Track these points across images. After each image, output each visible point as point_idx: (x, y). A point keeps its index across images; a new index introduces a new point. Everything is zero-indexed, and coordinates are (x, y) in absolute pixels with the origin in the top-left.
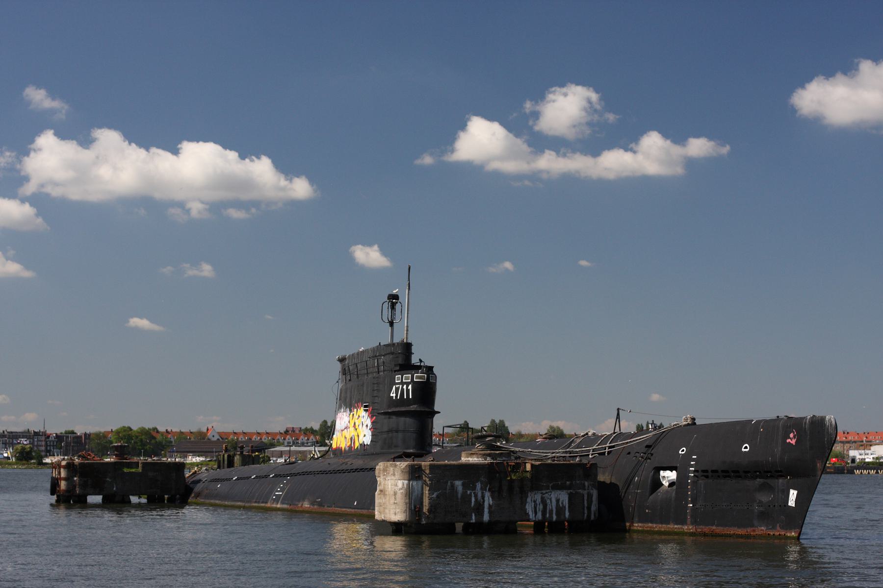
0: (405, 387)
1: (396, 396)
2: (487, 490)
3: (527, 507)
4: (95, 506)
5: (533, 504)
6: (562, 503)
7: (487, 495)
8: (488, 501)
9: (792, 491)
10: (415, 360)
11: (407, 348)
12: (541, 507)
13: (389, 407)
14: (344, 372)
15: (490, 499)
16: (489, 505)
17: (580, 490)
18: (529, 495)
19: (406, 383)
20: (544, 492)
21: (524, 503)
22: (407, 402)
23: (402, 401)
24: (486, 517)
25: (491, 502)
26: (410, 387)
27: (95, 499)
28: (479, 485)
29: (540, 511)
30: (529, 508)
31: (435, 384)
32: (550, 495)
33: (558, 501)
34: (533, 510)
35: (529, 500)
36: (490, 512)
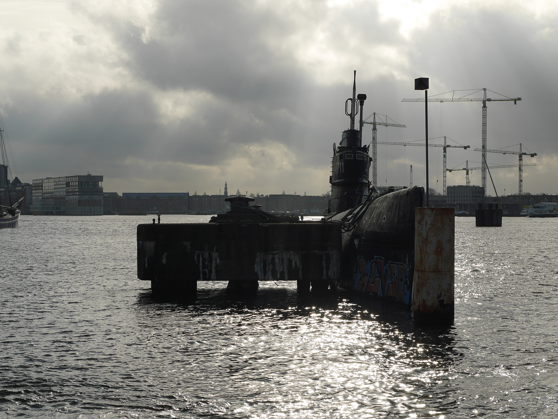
2: (215, 251)
3: (256, 266)
5: (262, 264)
6: (296, 263)
7: (215, 255)
12: (271, 267)
15: (218, 259)
16: (216, 264)
17: (315, 251)
18: (258, 255)
20: (275, 252)
25: (218, 261)
29: (270, 270)
32: (282, 256)
33: (290, 261)
34: (262, 270)
35: (258, 260)
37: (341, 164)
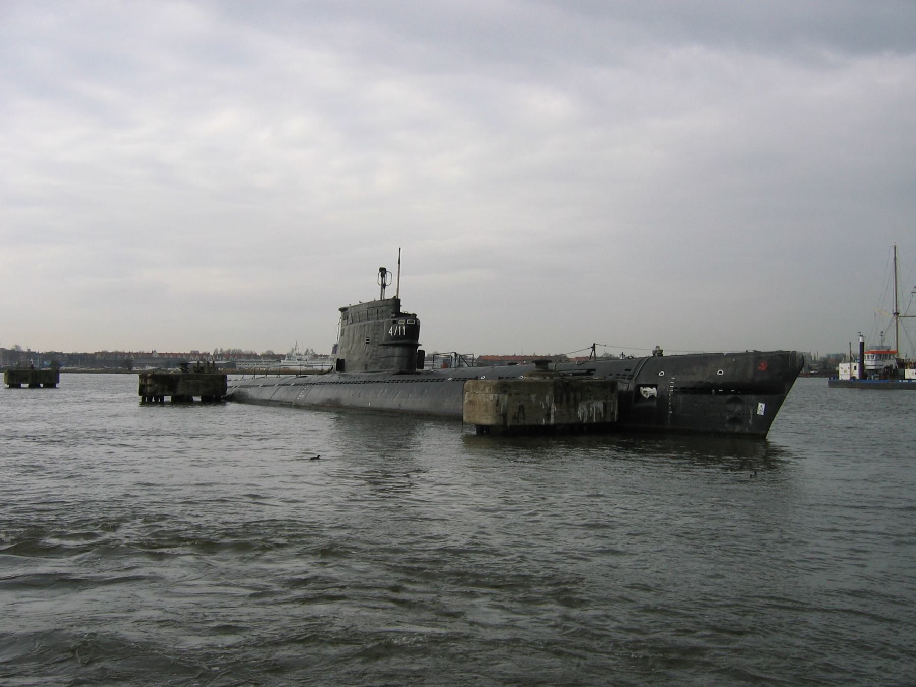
0: (400, 328)
1: (393, 334)
4: (168, 403)
8: (554, 408)
9: (760, 404)
10: (402, 311)
11: (396, 302)
13: (387, 340)
14: (345, 317)
19: (401, 325)
21: (576, 410)
22: (402, 337)
23: (397, 337)
24: (552, 421)
26: (404, 328)
27: (168, 399)
28: (547, 398)
30: (580, 414)
31: (419, 326)
35: (579, 408)
36: (554, 418)
37: (402, 328)
